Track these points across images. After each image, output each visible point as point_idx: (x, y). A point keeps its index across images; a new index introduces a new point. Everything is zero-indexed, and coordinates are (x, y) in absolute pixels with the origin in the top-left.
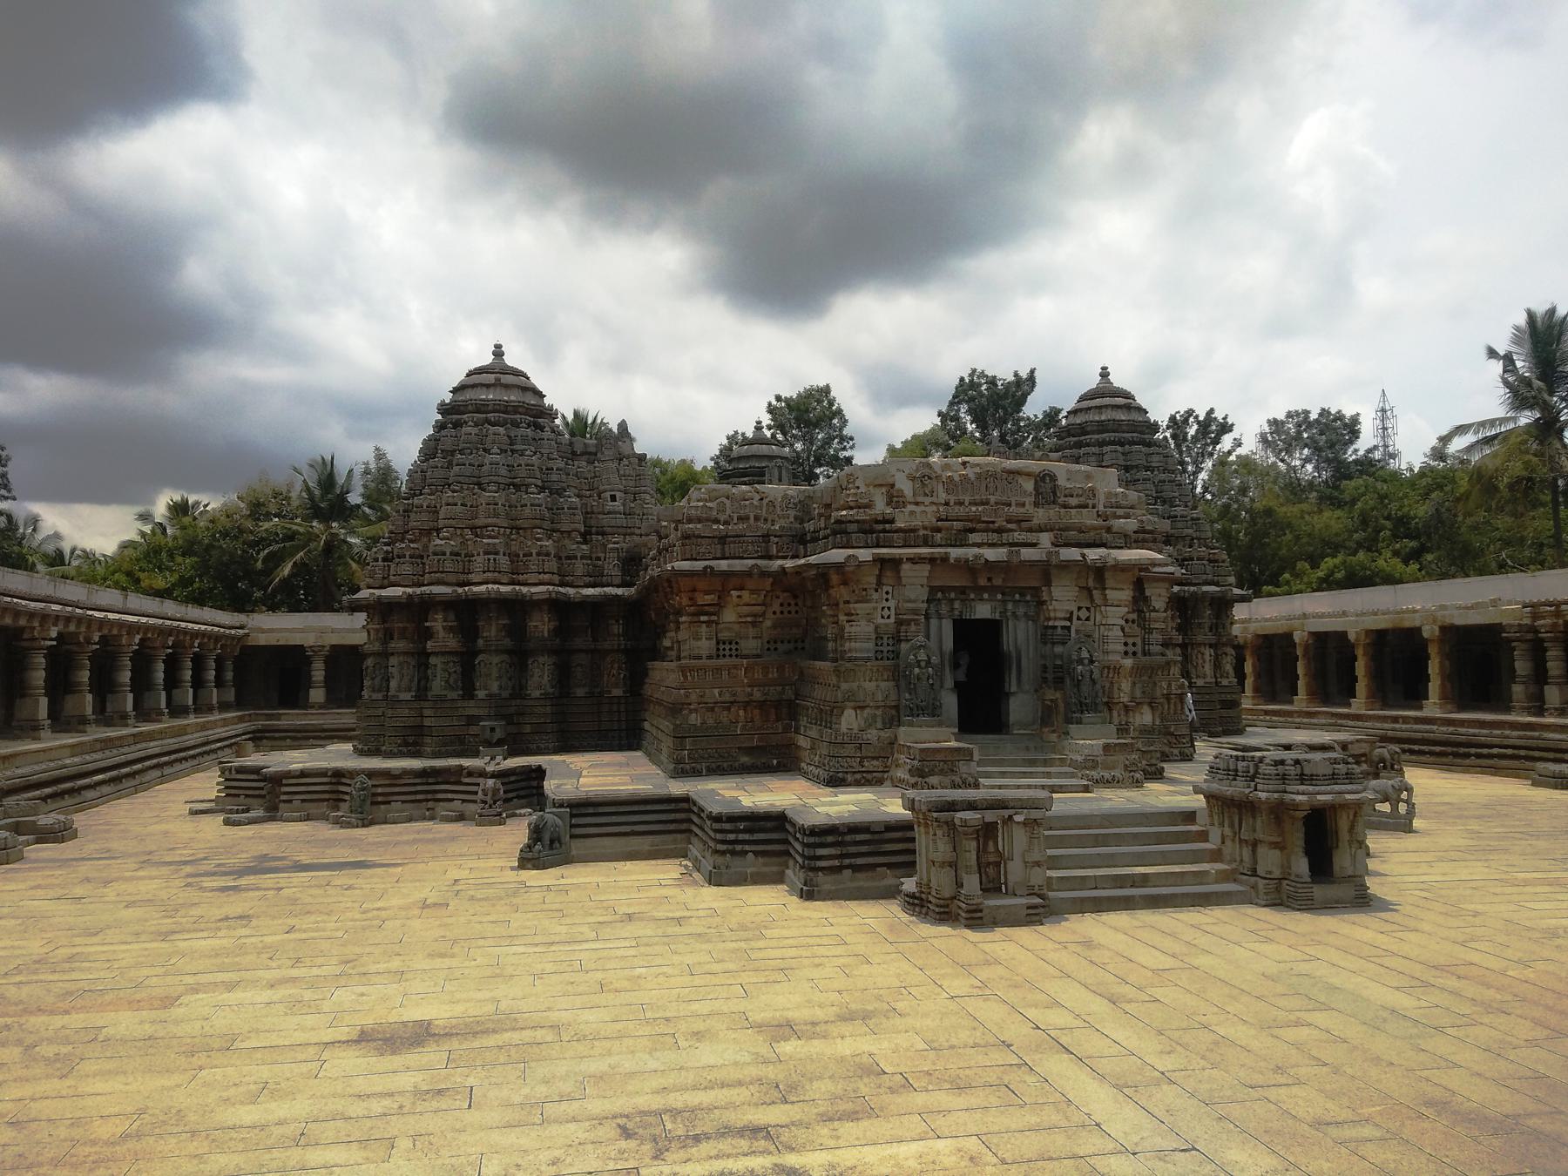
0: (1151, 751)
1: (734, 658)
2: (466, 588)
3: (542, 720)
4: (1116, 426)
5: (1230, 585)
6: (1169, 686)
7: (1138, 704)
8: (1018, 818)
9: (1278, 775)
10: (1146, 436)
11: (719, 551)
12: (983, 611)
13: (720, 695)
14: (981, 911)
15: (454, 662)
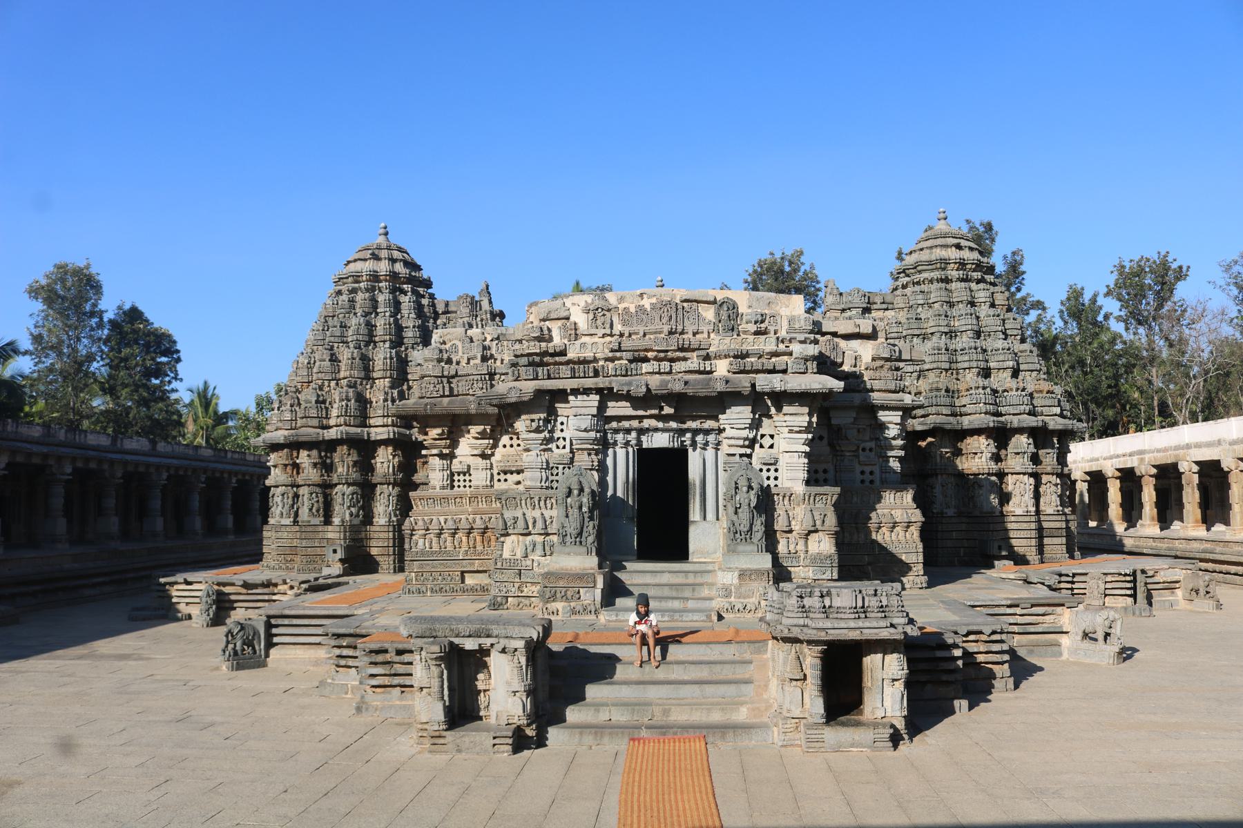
0: (824, 580)
1: (462, 488)
2: (325, 431)
3: (386, 544)
4: (944, 264)
5: (1056, 415)
6: (902, 515)
7: (810, 532)
8: (499, 647)
9: (803, 607)
10: (976, 273)
11: (447, 389)
12: (660, 440)
13: (445, 523)
14: (444, 737)
15: (317, 493)
